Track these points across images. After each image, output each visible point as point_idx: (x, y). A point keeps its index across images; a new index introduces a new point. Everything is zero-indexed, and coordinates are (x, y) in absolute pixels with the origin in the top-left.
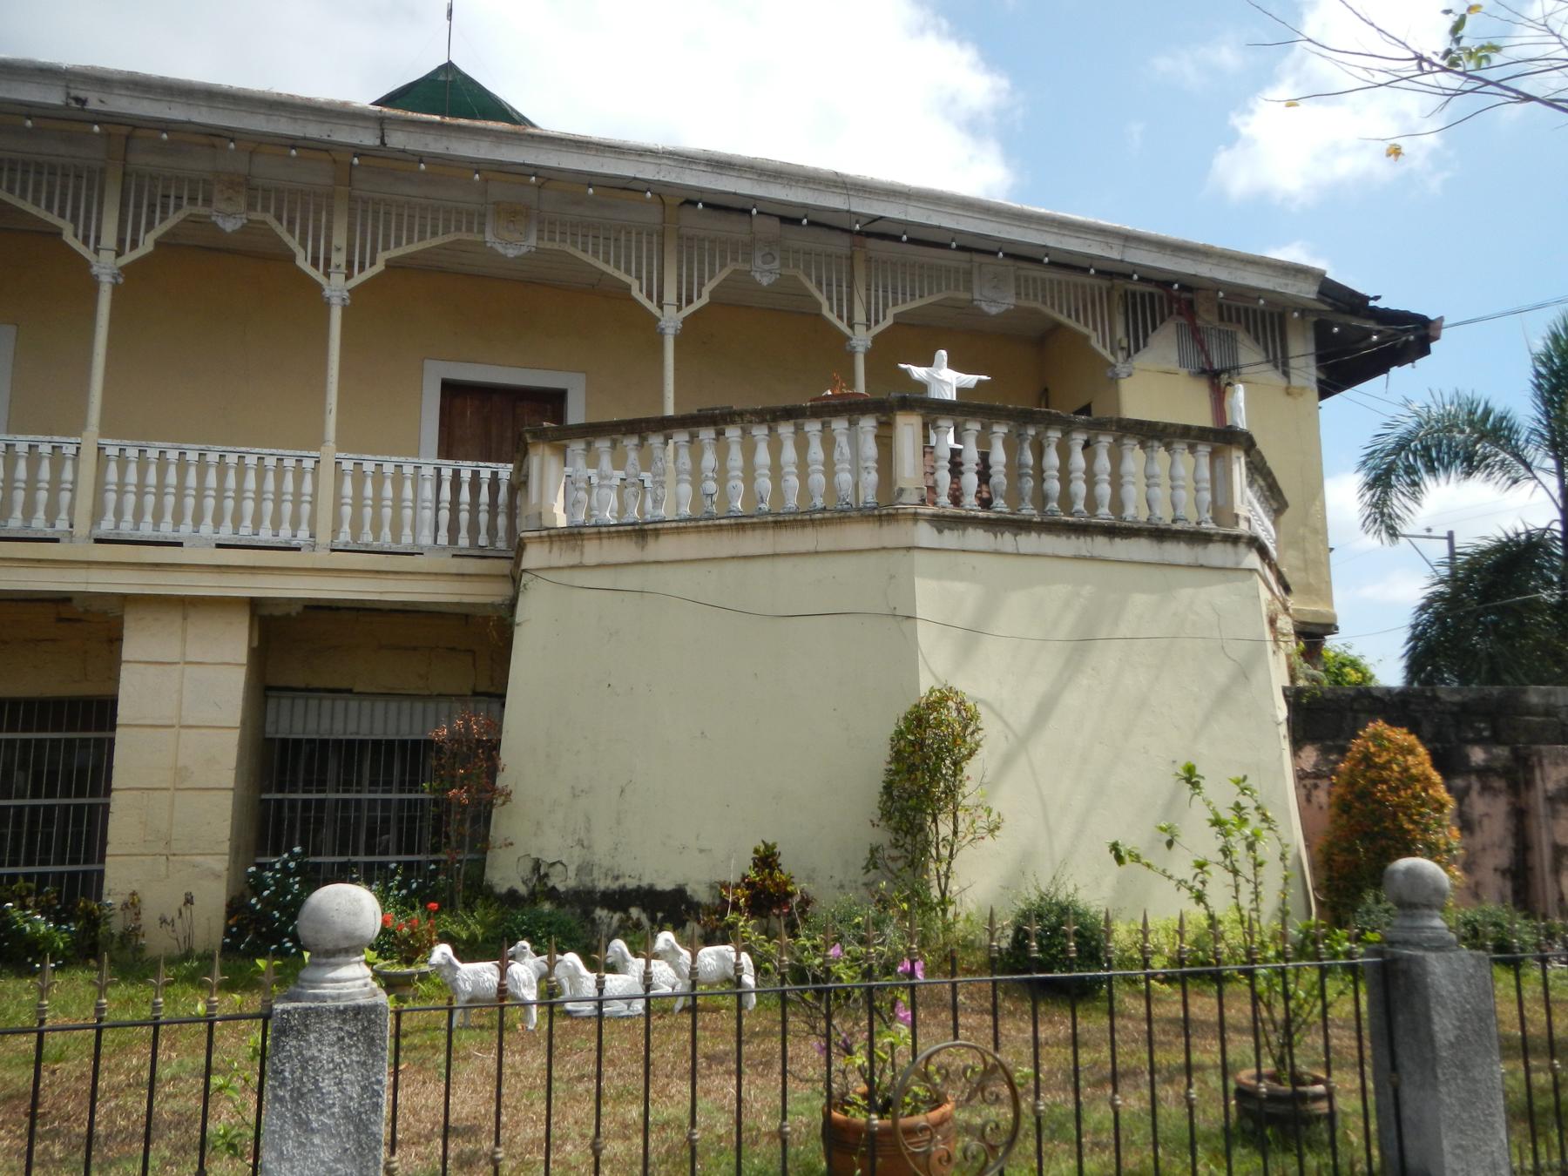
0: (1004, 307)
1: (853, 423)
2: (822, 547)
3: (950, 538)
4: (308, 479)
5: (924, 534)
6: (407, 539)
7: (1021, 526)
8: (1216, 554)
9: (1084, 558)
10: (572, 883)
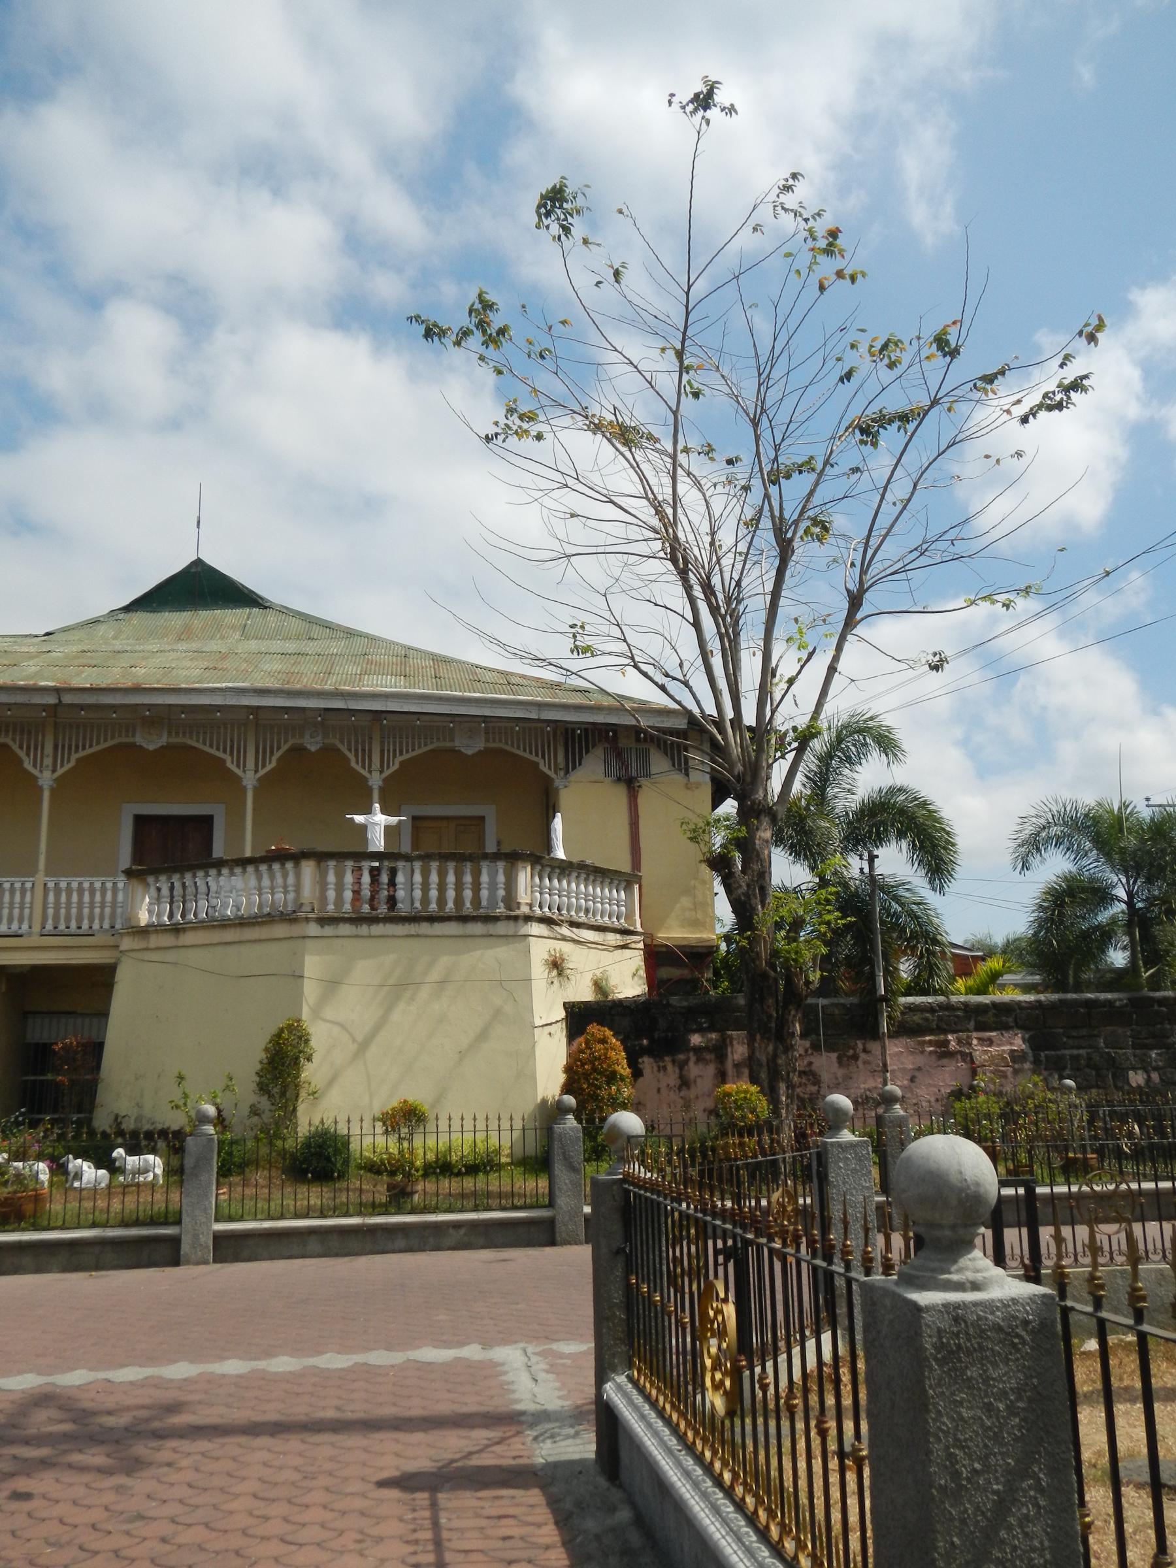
0: (477, 750)
1: (283, 865)
2: (263, 937)
3: (329, 930)
4: (28, 894)
5: (313, 929)
6: (85, 926)
7: (372, 920)
8: (501, 928)
9: (412, 936)
10: (132, 1127)
